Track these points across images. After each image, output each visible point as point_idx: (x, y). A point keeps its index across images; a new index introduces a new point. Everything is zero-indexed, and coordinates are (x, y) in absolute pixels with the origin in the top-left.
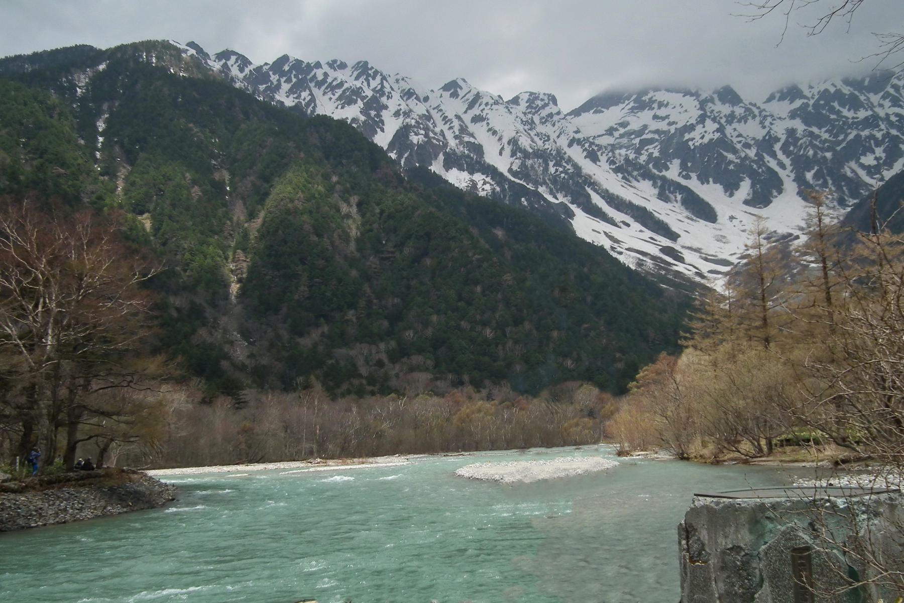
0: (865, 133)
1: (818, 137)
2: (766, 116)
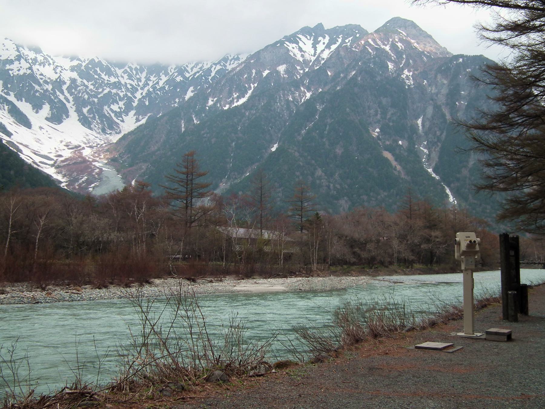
0: (114, 91)
1: (87, 87)
2: (57, 66)
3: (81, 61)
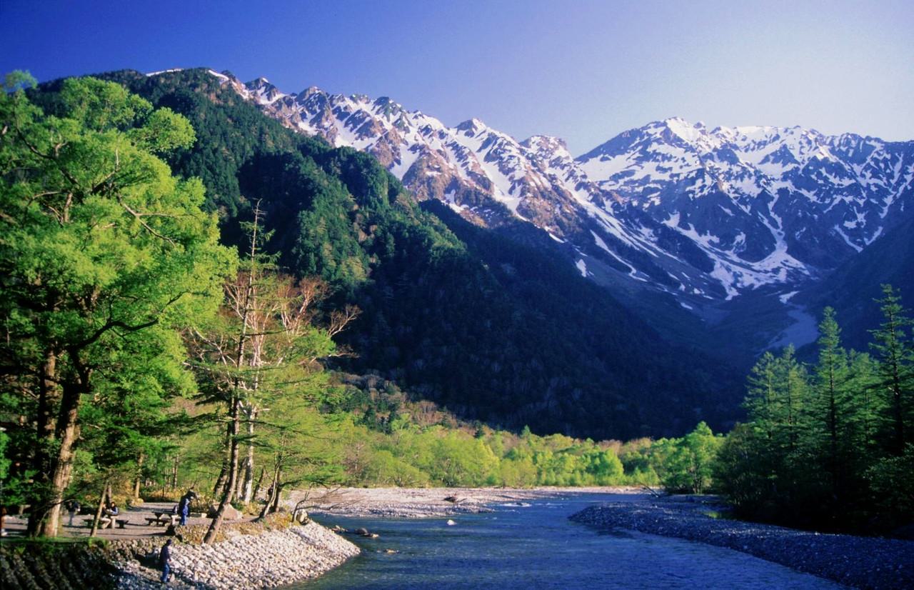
0: (849, 199)
3: (799, 163)
